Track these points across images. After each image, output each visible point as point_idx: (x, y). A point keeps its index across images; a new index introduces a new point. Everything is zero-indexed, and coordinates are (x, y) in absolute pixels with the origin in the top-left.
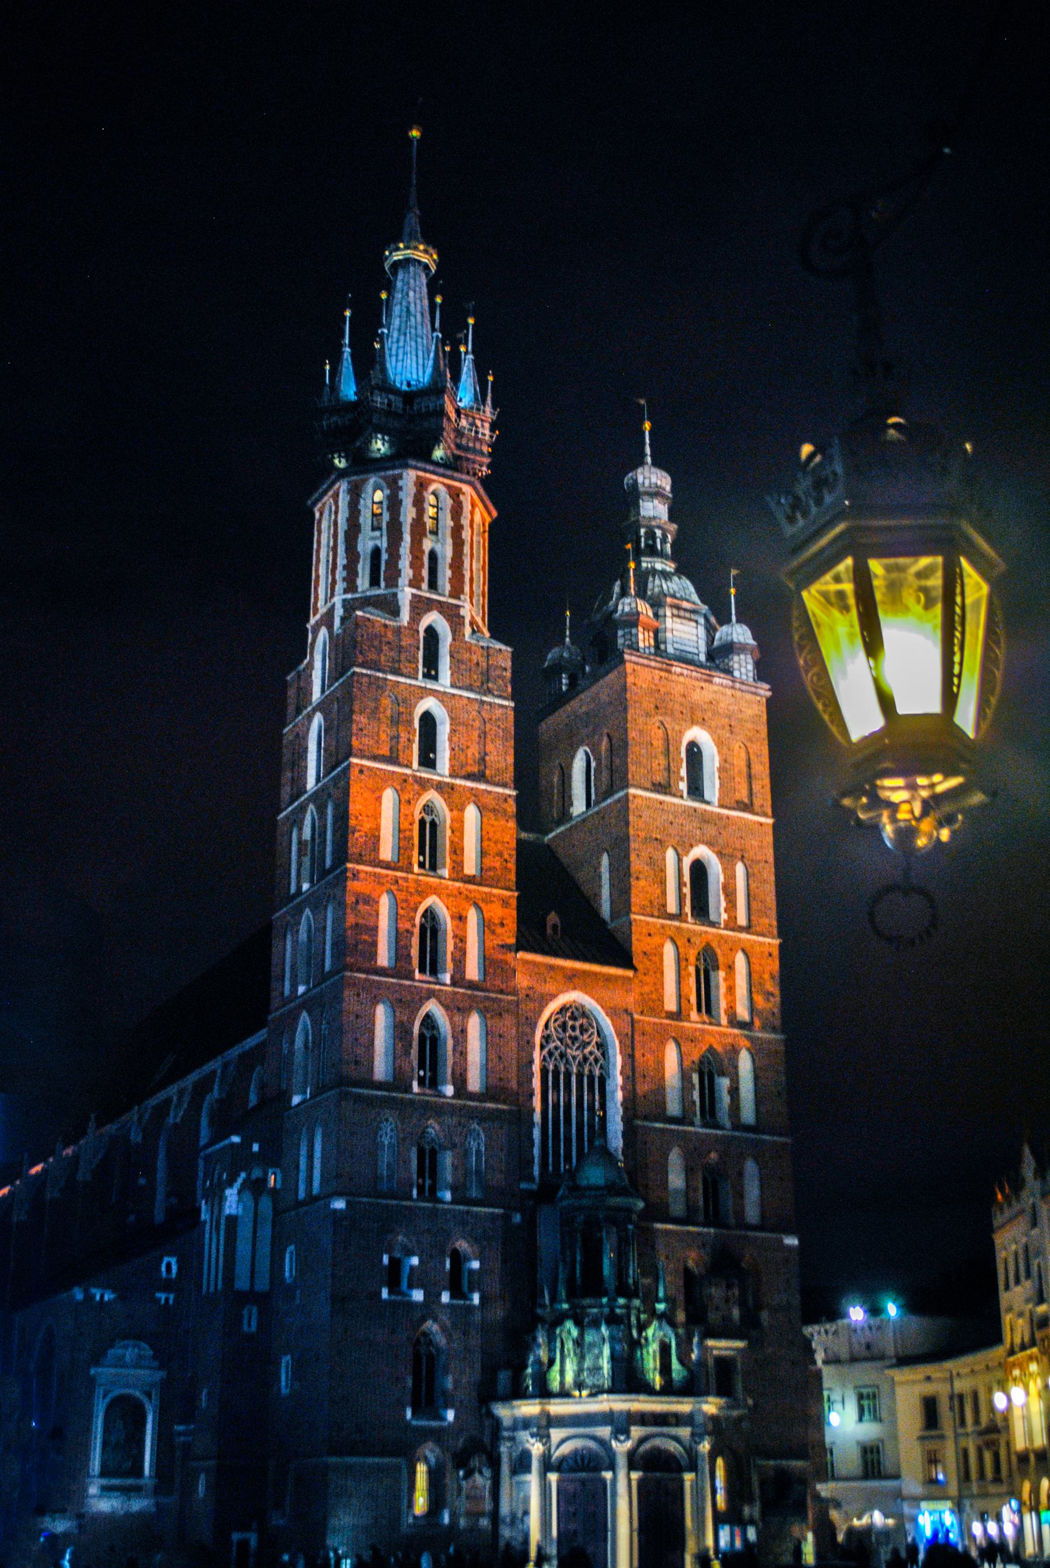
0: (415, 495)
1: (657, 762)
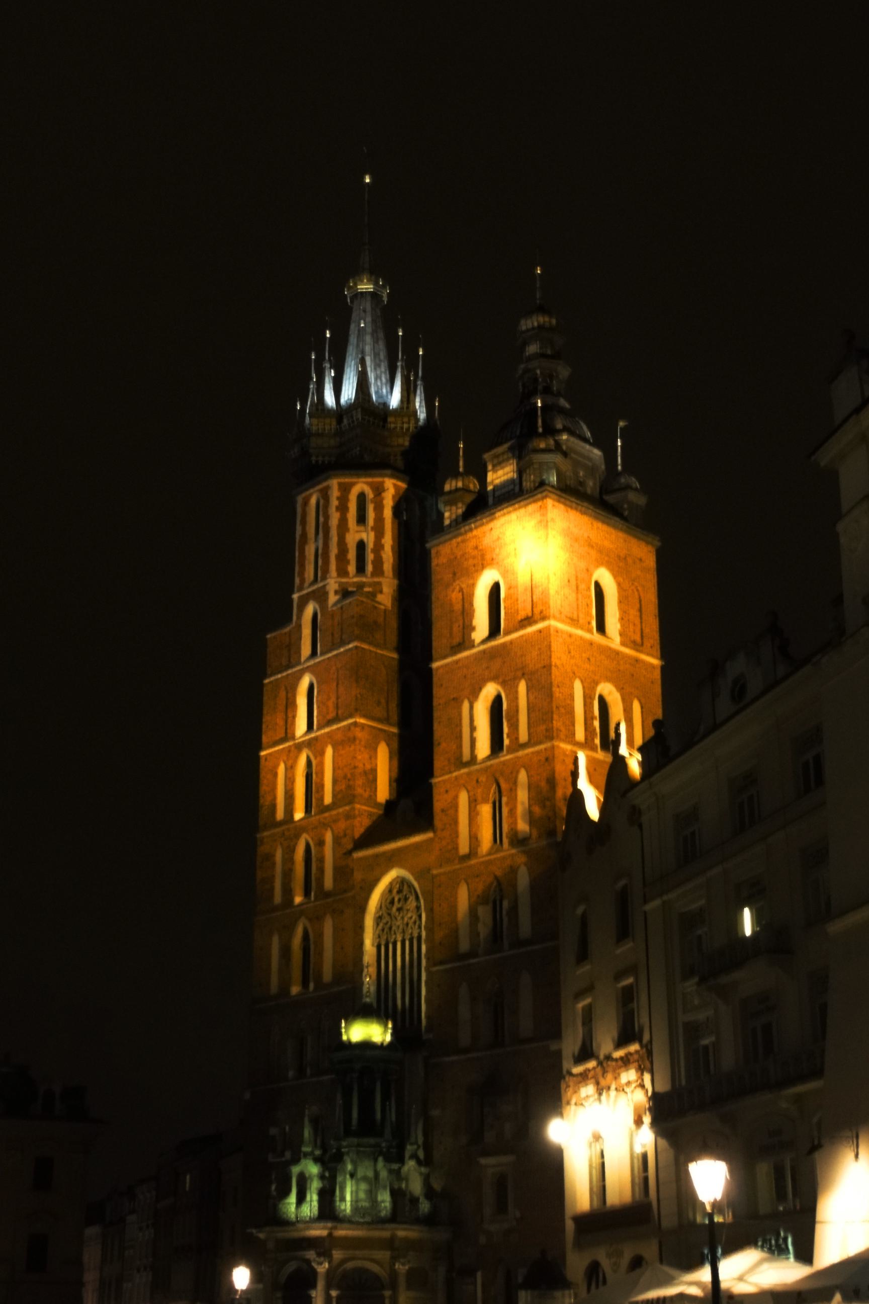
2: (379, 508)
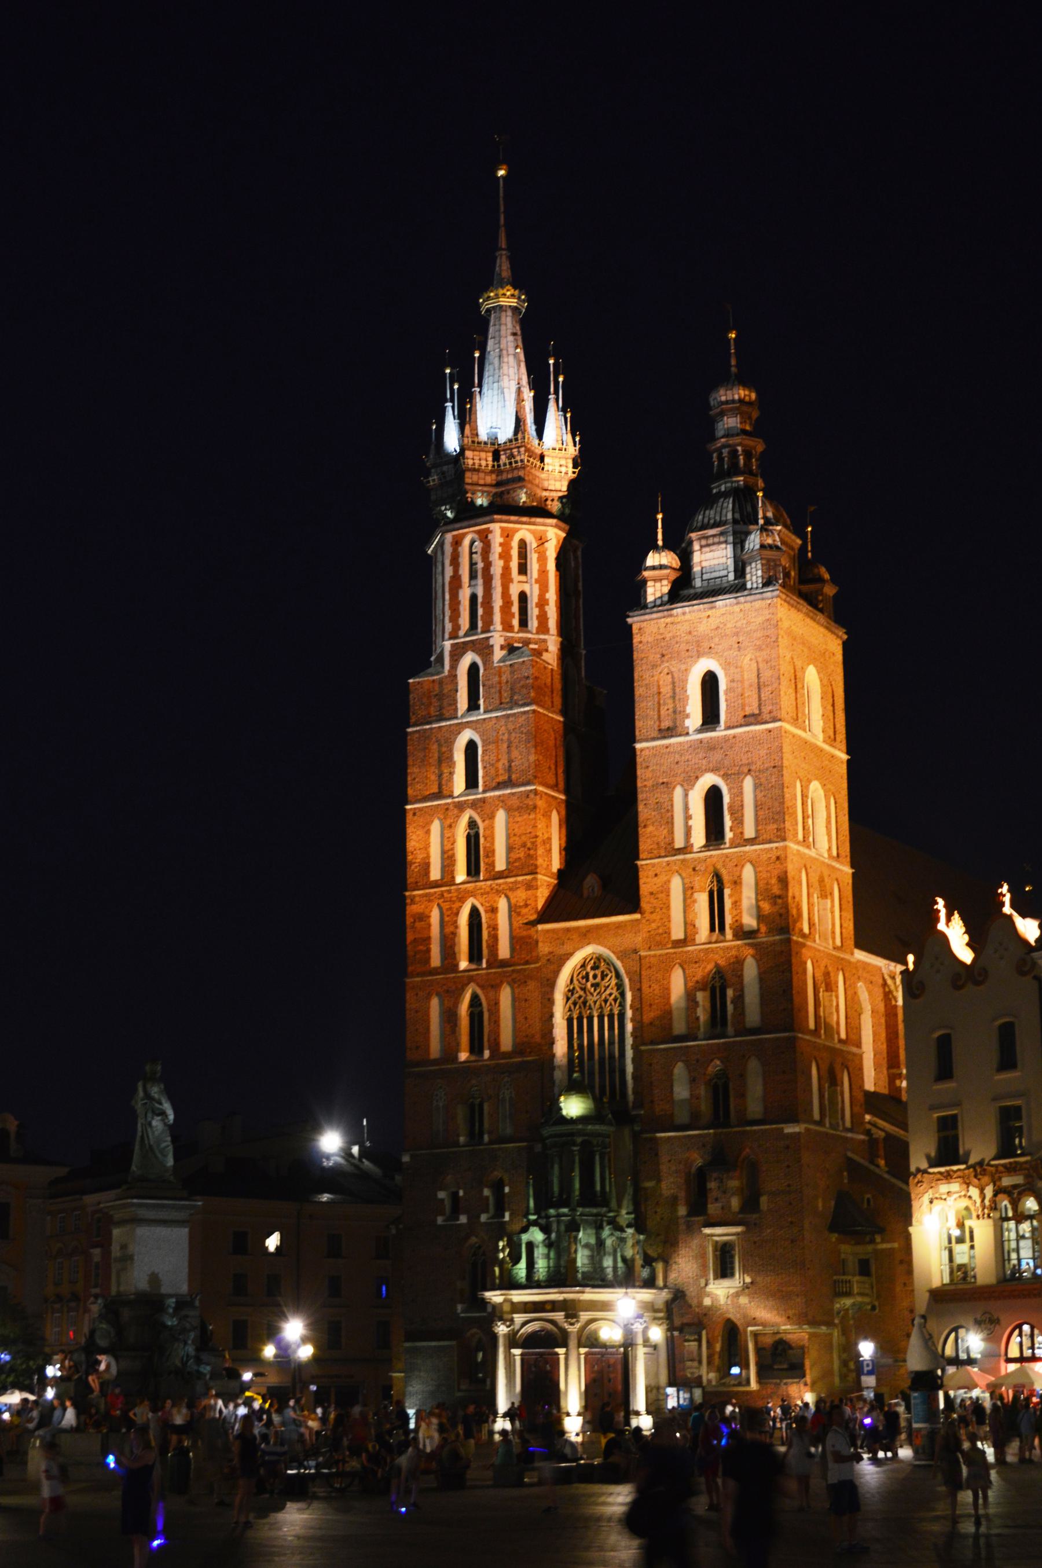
0: (452, 554)
1: (666, 708)
2: (542, 559)
